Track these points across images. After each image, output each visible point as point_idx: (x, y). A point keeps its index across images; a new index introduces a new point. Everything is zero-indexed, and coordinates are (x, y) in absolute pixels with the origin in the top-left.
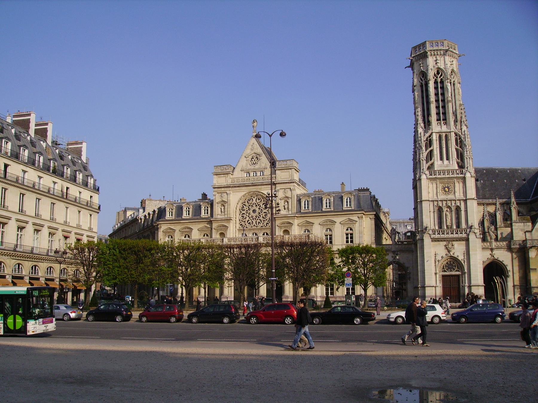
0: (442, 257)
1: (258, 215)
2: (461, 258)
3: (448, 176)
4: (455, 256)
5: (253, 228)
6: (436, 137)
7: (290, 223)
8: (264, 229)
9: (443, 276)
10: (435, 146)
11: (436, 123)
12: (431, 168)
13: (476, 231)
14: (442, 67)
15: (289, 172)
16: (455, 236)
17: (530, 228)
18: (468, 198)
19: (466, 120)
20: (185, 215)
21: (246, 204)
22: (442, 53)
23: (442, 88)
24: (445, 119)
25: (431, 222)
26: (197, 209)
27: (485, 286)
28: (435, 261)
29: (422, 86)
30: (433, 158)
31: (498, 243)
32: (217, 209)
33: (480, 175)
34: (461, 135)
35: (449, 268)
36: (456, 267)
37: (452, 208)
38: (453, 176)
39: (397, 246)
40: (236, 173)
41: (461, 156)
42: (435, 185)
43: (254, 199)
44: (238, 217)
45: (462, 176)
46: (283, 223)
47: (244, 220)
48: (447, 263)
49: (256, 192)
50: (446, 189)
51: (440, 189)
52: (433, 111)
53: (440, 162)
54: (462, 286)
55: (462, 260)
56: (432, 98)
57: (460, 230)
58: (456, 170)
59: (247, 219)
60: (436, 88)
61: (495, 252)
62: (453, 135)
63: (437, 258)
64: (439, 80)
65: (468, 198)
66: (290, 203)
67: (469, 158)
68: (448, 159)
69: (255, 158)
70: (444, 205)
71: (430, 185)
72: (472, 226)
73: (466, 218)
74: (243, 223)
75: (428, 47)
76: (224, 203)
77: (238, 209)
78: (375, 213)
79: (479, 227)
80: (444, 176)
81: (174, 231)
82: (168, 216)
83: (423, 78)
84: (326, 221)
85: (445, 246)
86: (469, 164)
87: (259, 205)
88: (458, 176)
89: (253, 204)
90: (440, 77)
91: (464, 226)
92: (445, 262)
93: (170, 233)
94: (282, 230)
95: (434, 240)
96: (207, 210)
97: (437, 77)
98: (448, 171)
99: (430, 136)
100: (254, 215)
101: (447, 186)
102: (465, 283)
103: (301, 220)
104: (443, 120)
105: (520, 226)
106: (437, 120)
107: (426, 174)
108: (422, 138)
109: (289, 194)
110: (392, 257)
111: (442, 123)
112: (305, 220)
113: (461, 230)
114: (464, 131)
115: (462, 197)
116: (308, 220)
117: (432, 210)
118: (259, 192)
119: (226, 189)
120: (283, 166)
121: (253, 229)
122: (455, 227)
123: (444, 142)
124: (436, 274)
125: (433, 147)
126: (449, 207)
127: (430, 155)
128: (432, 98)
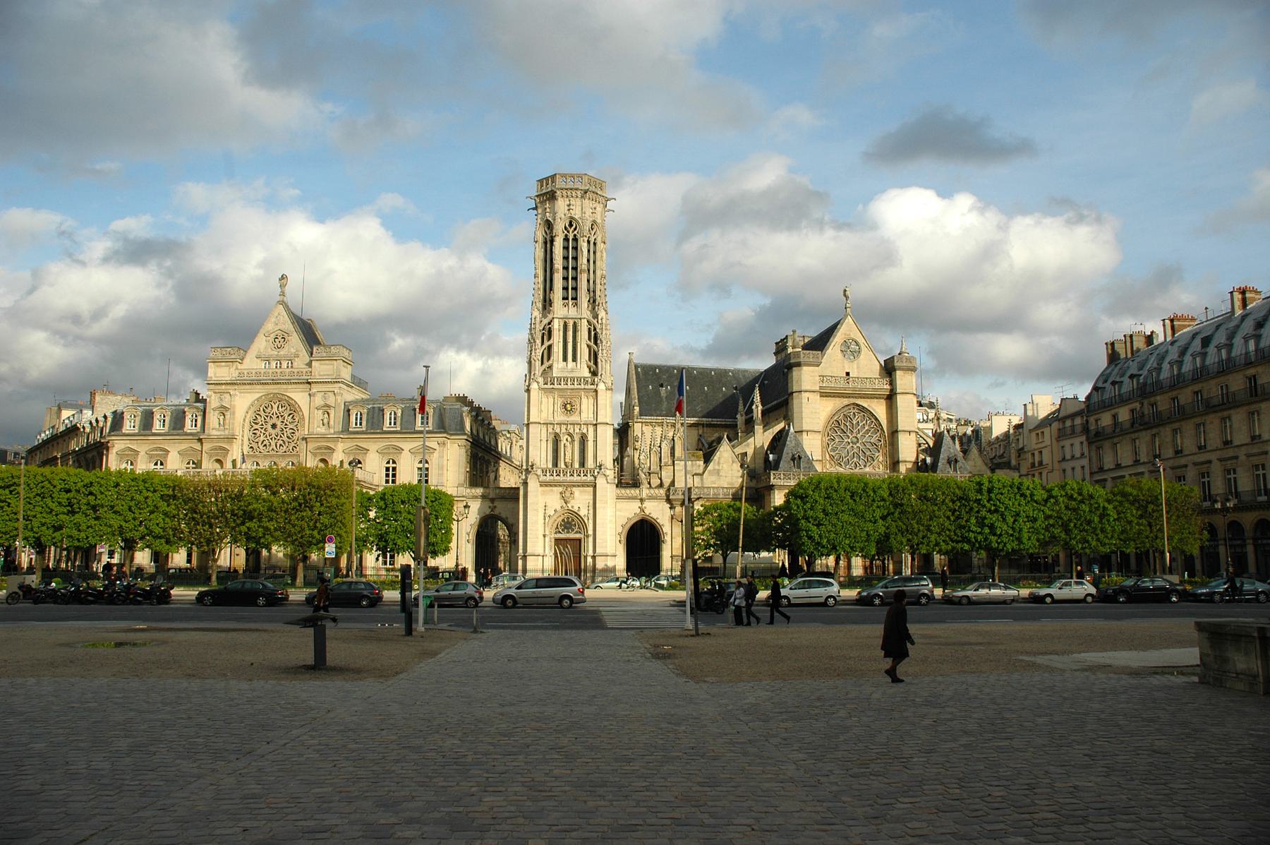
1: (280, 433)
2: (583, 513)
4: (576, 509)
5: (271, 453)
7: (329, 448)
8: (289, 456)
9: (556, 540)
13: (608, 472)
14: (576, 217)
15: (333, 365)
16: (576, 478)
18: (599, 421)
20: (157, 426)
21: (262, 413)
22: (579, 195)
23: (575, 248)
24: (575, 299)
26: (178, 420)
29: (546, 243)
30: (552, 358)
31: (652, 491)
32: (213, 419)
33: (668, 377)
37: (575, 436)
39: (498, 491)
40: (247, 361)
41: (594, 357)
42: (551, 400)
43: (275, 407)
44: (248, 434)
45: (592, 387)
46: (319, 448)
47: (256, 440)
48: (563, 520)
53: (562, 364)
56: (559, 263)
58: (584, 378)
59: (262, 438)
60: (566, 248)
61: (647, 504)
62: (585, 322)
64: (571, 238)
65: (599, 421)
66: (332, 416)
68: (574, 359)
69: (280, 338)
70: (564, 430)
71: (543, 399)
74: (254, 445)
75: (560, 183)
76: (223, 410)
77: (247, 420)
81: (137, 453)
82: (128, 427)
83: (549, 228)
84: (388, 447)
85: (561, 493)
88: (586, 387)
90: (573, 232)
91: (590, 463)
92: (561, 519)
93: (131, 456)
94: (318, 459)
95: (543, 484)
96: (196, 421)
97: (568, 232)
98: (573, 379)
99: (549, 324)
100: (273, 432)
102: (588, 551)
103: (349, 444)
104: (572, 299)
106: (564, 299)
107: (538, 382)
108: (537, 326)
109: (331, 400)
110: (490, 507)
111: (570, 303)
115: (591, 418)
117: (544, 437)
119: (228, 387)
120: (325, 355)
121: (271, 456)
122: (577, 465)
123: (570, 334)
124: (544, 536)
126: (570, 435)
128: (559, 263)
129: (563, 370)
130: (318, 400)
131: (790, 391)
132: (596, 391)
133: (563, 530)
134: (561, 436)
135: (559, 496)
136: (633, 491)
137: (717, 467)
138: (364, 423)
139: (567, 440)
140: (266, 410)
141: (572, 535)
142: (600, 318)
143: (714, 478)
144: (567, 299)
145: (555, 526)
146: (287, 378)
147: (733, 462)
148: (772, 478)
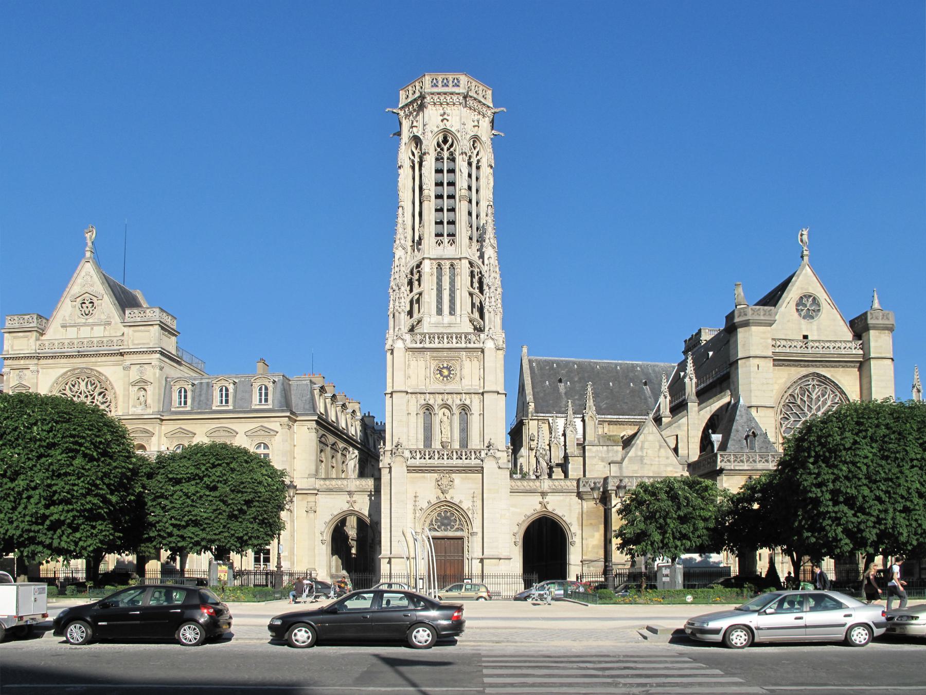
2: (465, 506)
4: (456, 501)
7: (146, 431)
10: (428, 285)
13: (498, 454)
16: (455, 462)
17: (619, 458)
28: (415, 510)
35: (443, 524)
36: (458, 522)
37: (454, 408)
38: (459, 345)
43: (83, 384)
48: (439, 515)
49: (87, 369)
52: (430, 216)
53: (435, 319)
55: (468, 509)
57: (466, 452)
58: (466, 334)
66: (149, 392)
68: (452, 311)
78: (316, 418)
80: (440, 346)
86: (493, 324)
87: (91, 395)
88: (469, 346)
89: (81, 393)
91: (475, 442)
92: (434, 515)
95: (411, 469)
98: (450, 336)
101: (445, 366)
105: (601, 452)
112: (178, 426)
113: (468, 453)
115: (476, 386)
116: (183, 427)
118: (92, 369)
122: (456, 445)
126: (447, 406)
129: (437, 325)
130: (134, 374)
131: (732, 359)
132: (483, 351)
133: (439, 527)
134: (436, 407)
135: (434, 483)
137: (640, 453)
138: (189, 401)
140: (73, 389)
141: (450, 534)
142: (486, 257)
143: (635, 467)
144: (442, 235)
145: (428, 522)
146: (95, 348)
147: (660, 447)
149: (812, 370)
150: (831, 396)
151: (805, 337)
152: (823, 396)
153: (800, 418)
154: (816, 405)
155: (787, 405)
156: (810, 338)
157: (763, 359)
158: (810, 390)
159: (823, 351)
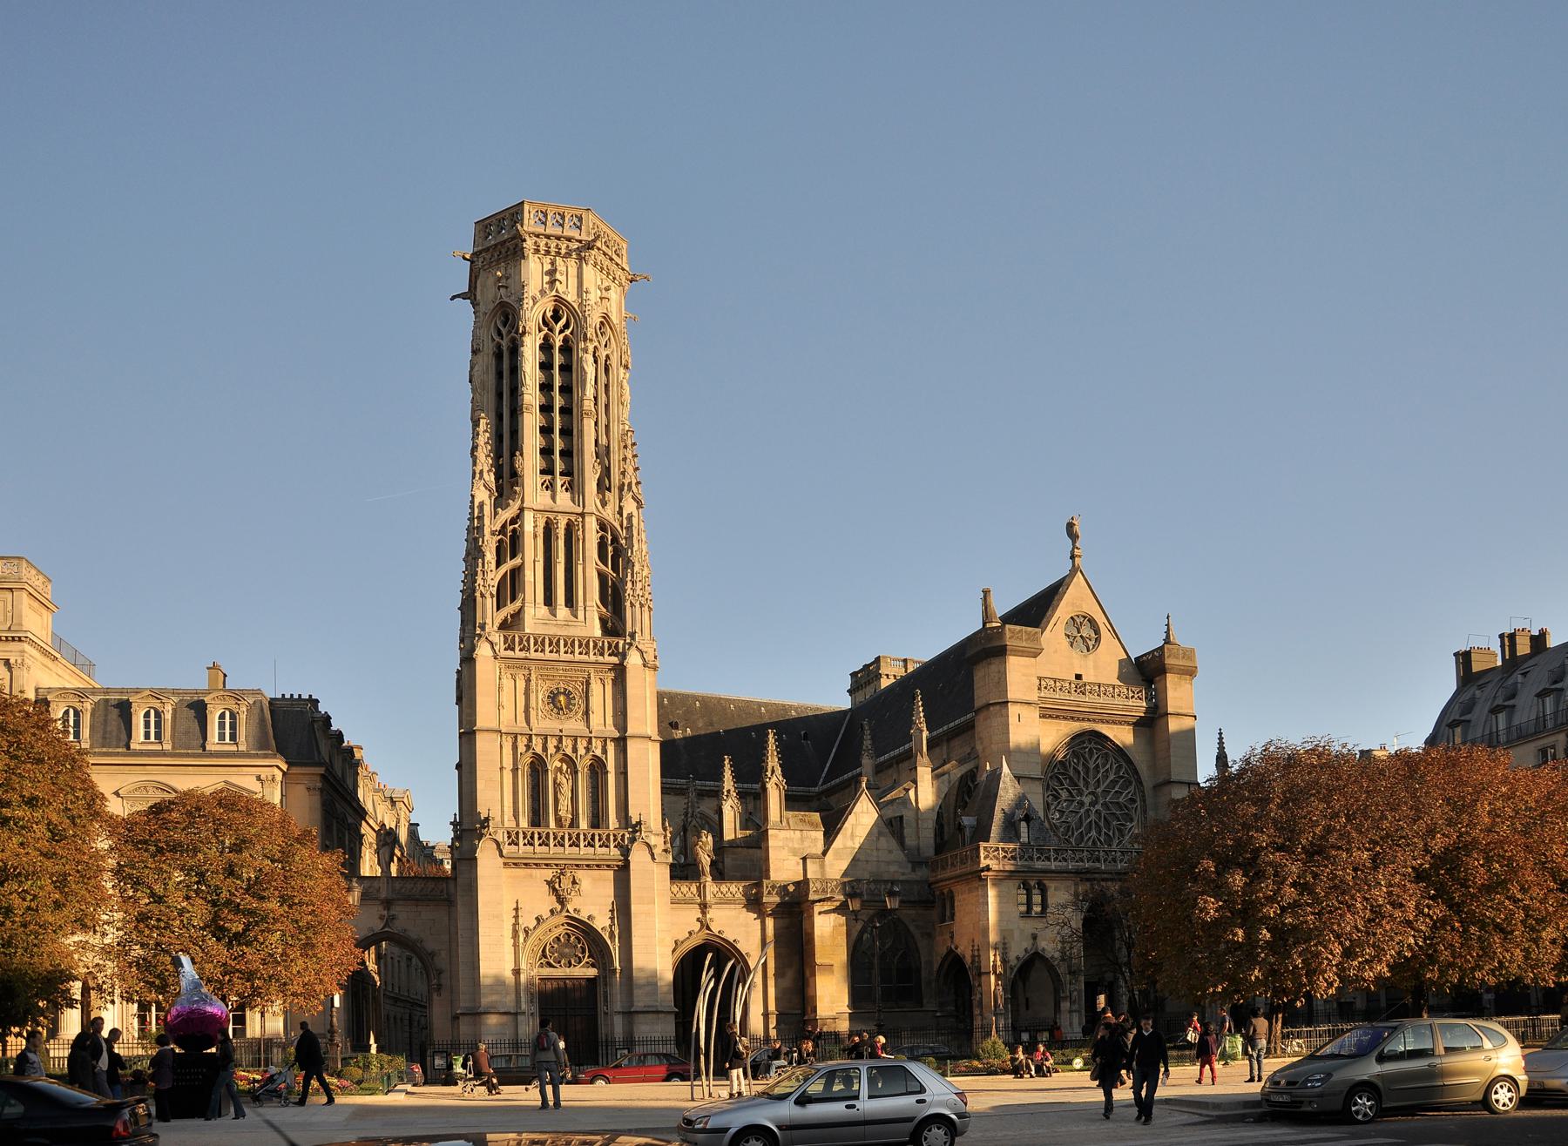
0: (537, 919)
2: (602, 922)
3: (569, 657)
4: (583, 916)
6: (535, 526)
11: (540, 481)
12: (512, 624)
13: (653, 840)
19: (638, 483)
25: (506, 803)
27: (677, 1014)
34: (619, 529)
35: (562, 955)
38: (584, 658)
41: (613, 597)
50: (562, 698)
51: (540, 697)
54: (606, 1014)
62: (592, 524)
63: (520, 921)
65: (630, 732)
67: (642, 605)
68: (570, 602)
70: (551, 750)
71: (504, 681)
72: (639, 823)
73: (623, 798)
79: (665, 829)
80: (554, 656)
86: (638, 625)
88: (600, 659)
91: (613, 822)
95: (514, 863)
110: (381, 917)
114: (630, 517)
122: (584, 824)
125: (523, 558)
127: (512, 586)
136: (684, 889)
139: (560, 770)
148: (982, 856)
149: (1087, 726)
150: (1115, 766)
151: (1078, 677)
152: (1104, 766)
153: (1073, 797)
154: (1094, 778)
155: (1055, 777)
156: (1085, 679)
157: (1026, 706)
158: (1087, 756)
159: (1104, 699)
